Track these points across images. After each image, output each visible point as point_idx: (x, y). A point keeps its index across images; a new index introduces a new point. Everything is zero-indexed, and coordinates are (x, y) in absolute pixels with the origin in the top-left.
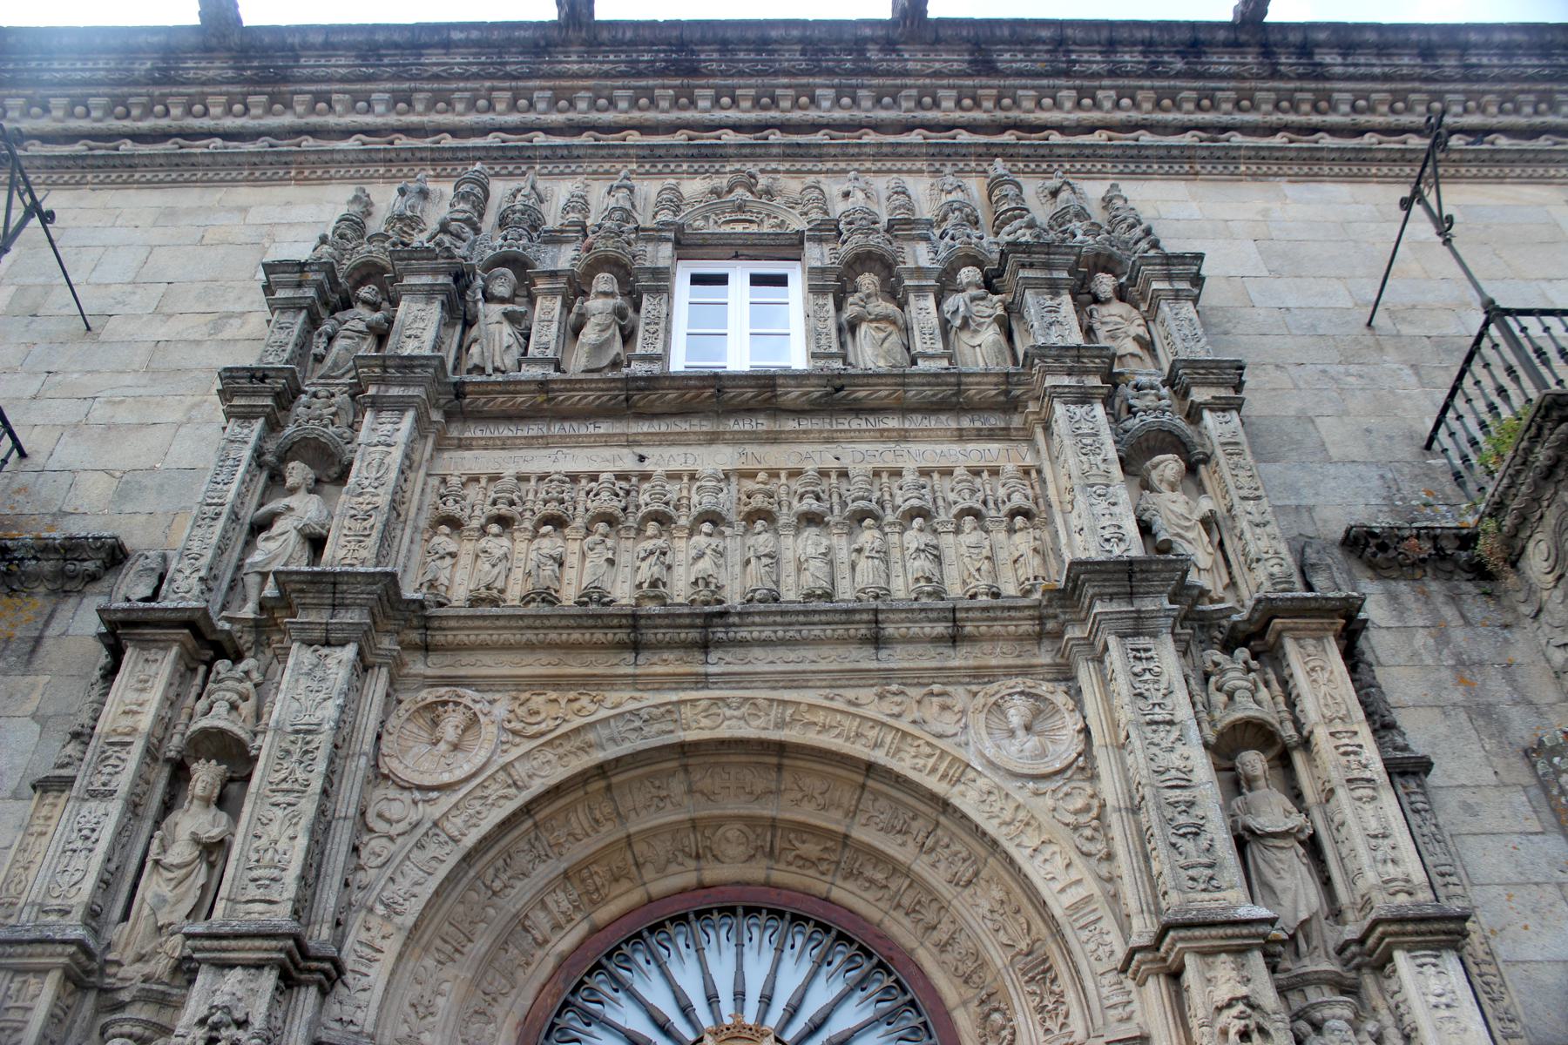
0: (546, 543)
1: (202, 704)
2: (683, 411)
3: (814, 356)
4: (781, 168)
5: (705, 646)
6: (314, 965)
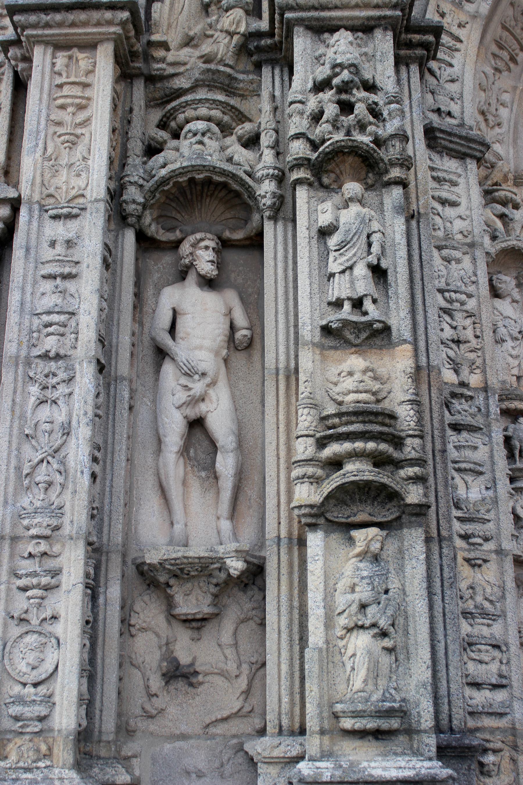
6: (416, 37)
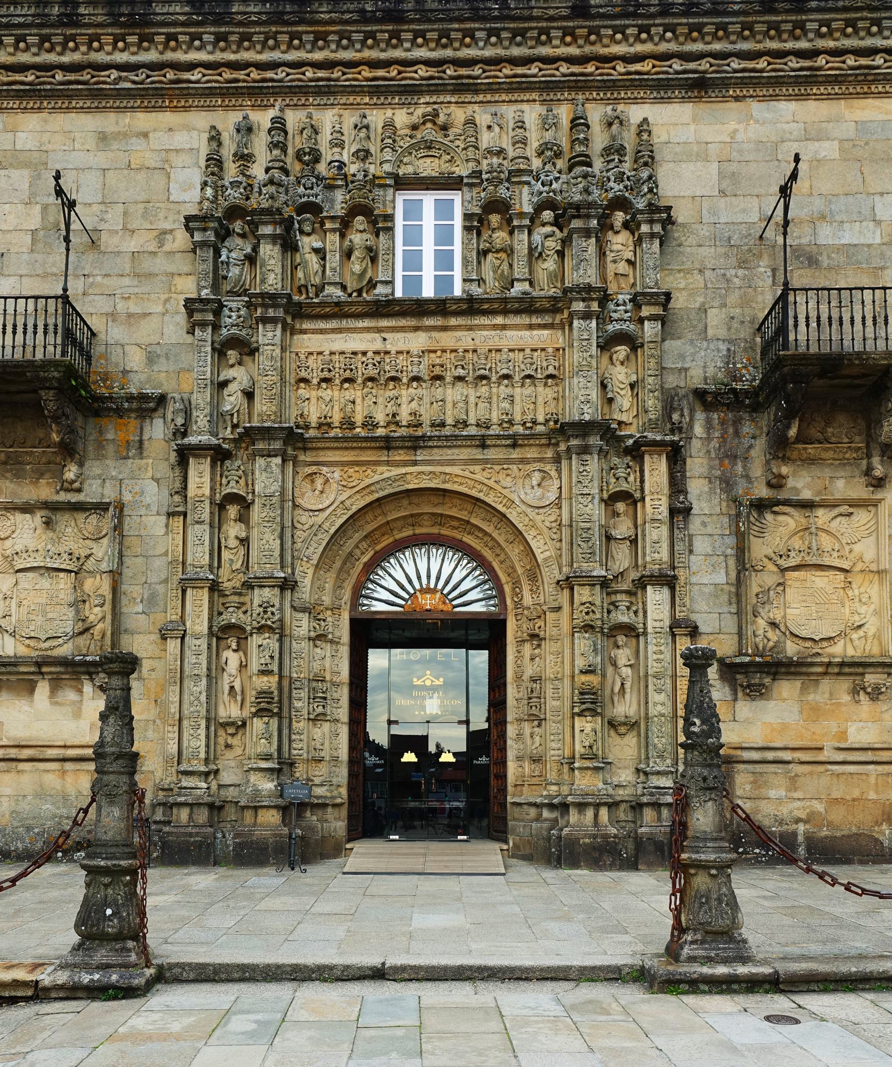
0: (347, 393)
1: (224, 481)
2: (403, 314)
3: (464, 280)
4: (453, 100)
5: (415, 448)
